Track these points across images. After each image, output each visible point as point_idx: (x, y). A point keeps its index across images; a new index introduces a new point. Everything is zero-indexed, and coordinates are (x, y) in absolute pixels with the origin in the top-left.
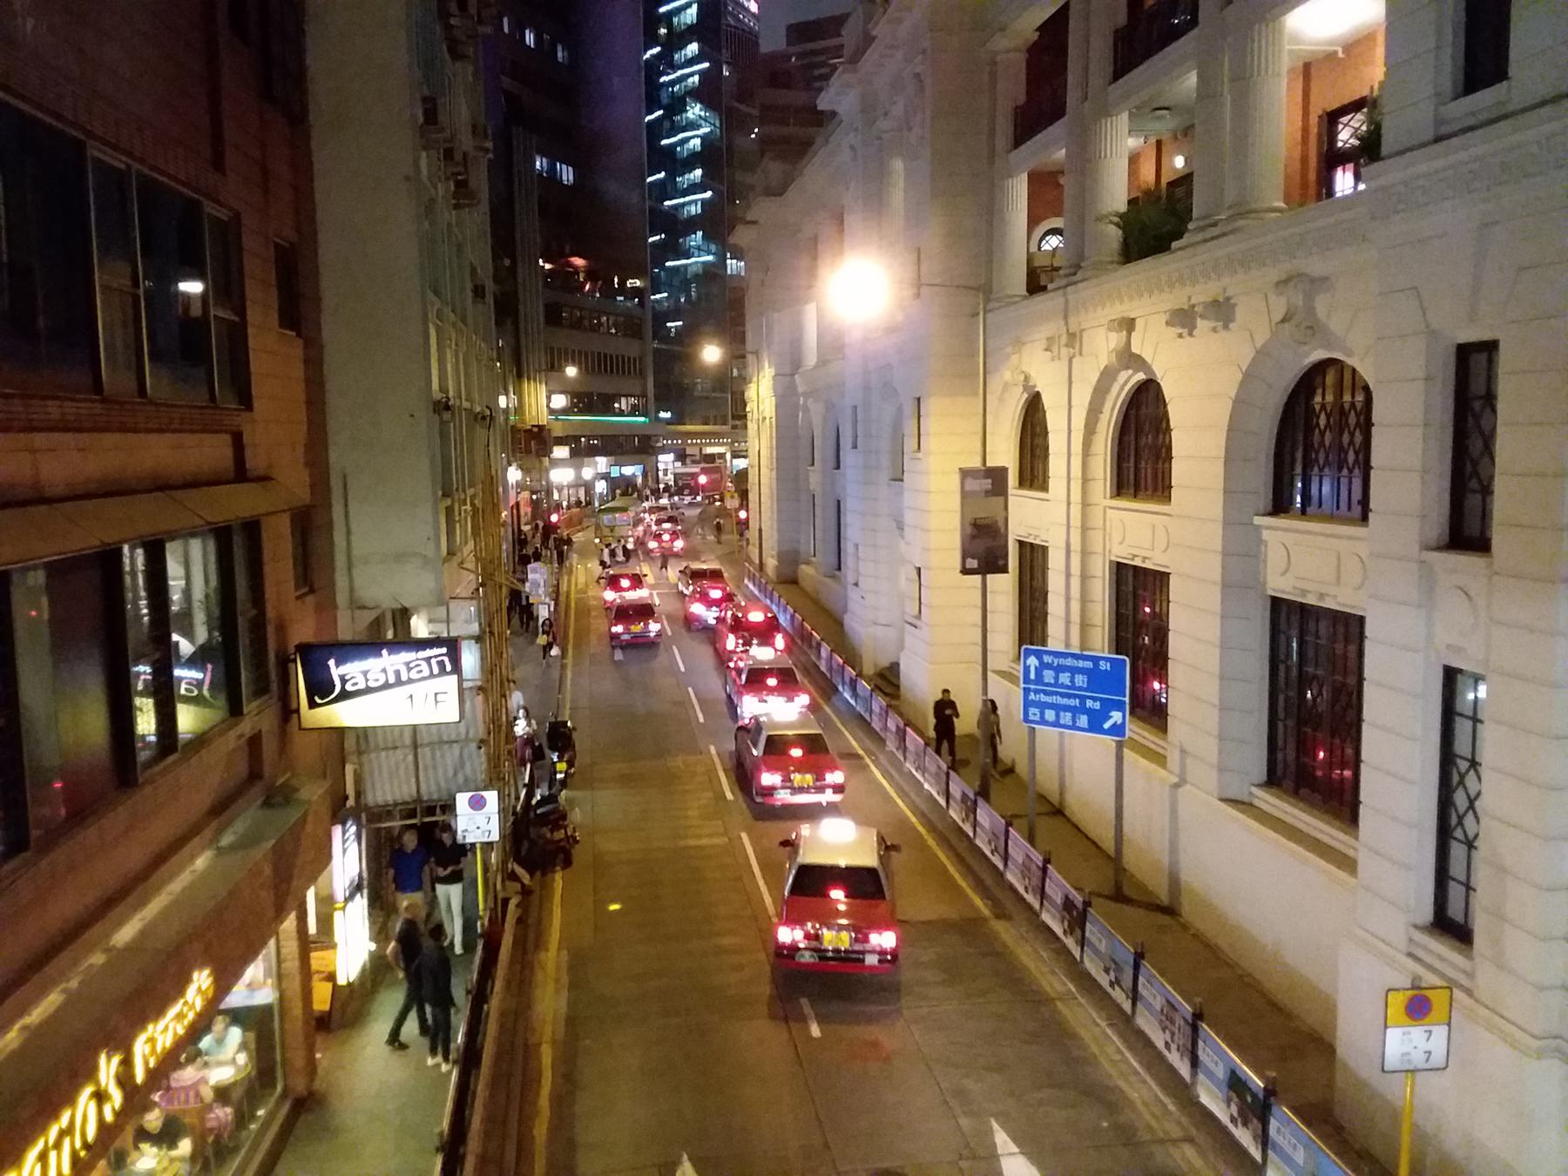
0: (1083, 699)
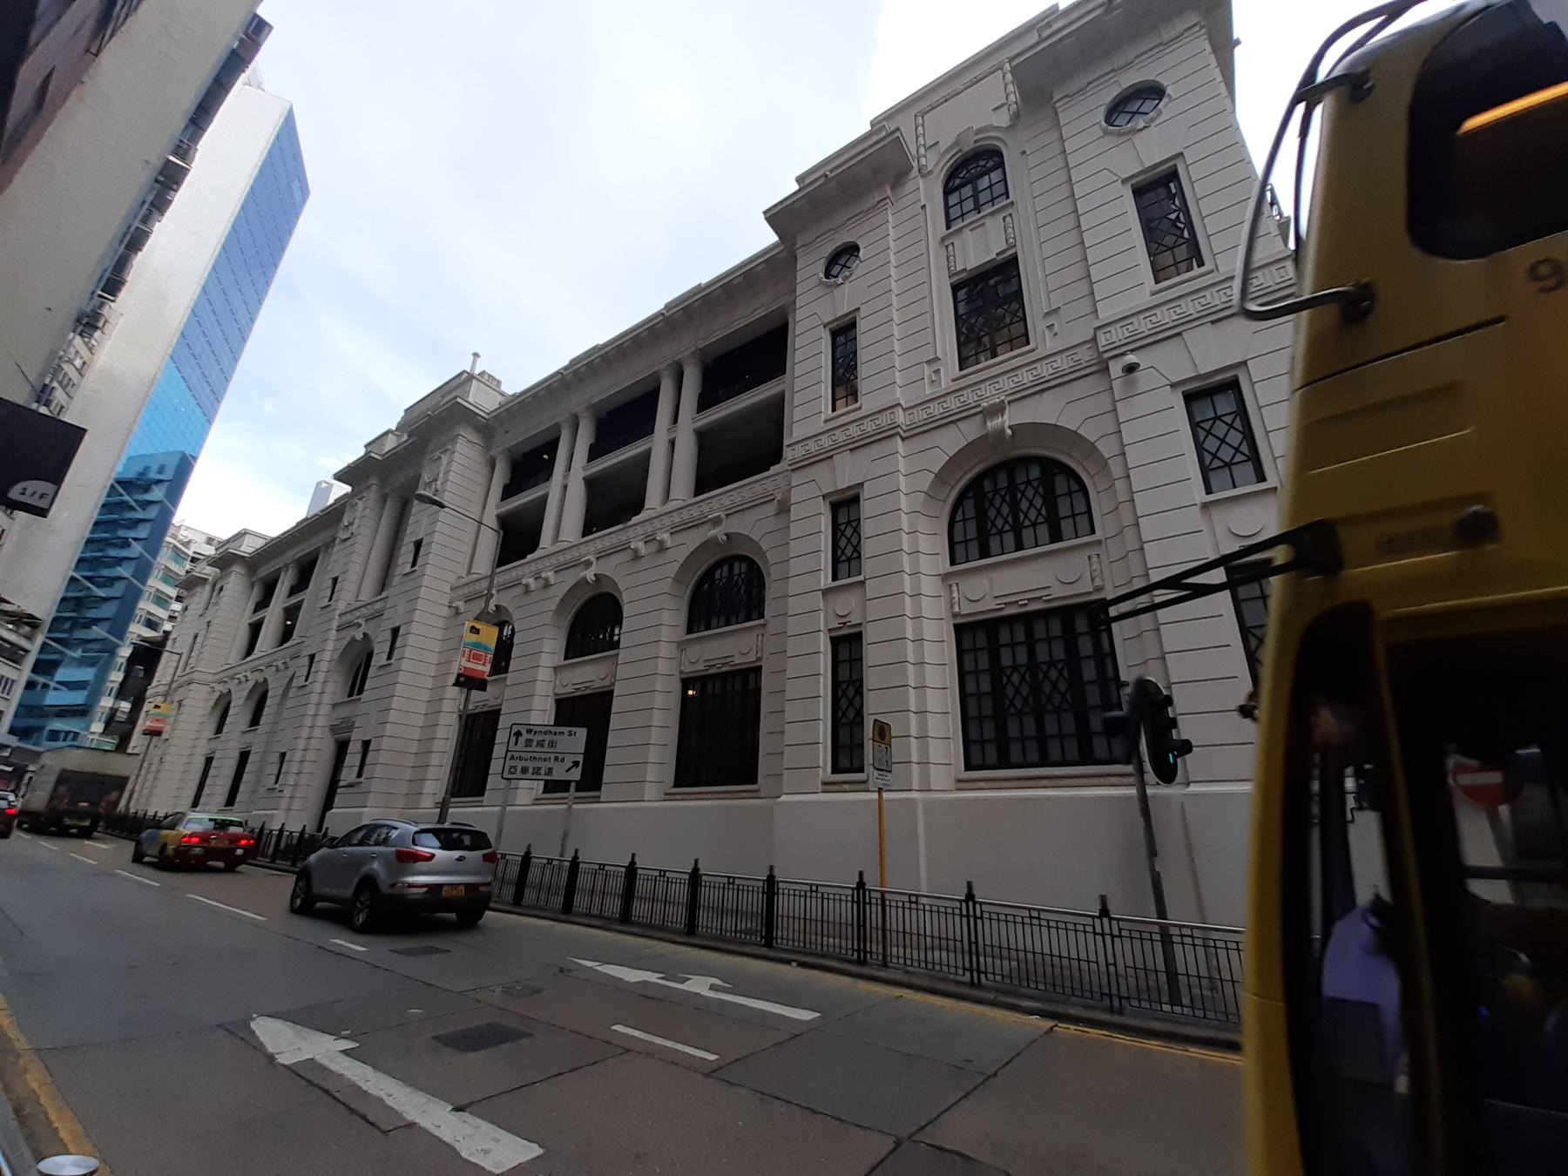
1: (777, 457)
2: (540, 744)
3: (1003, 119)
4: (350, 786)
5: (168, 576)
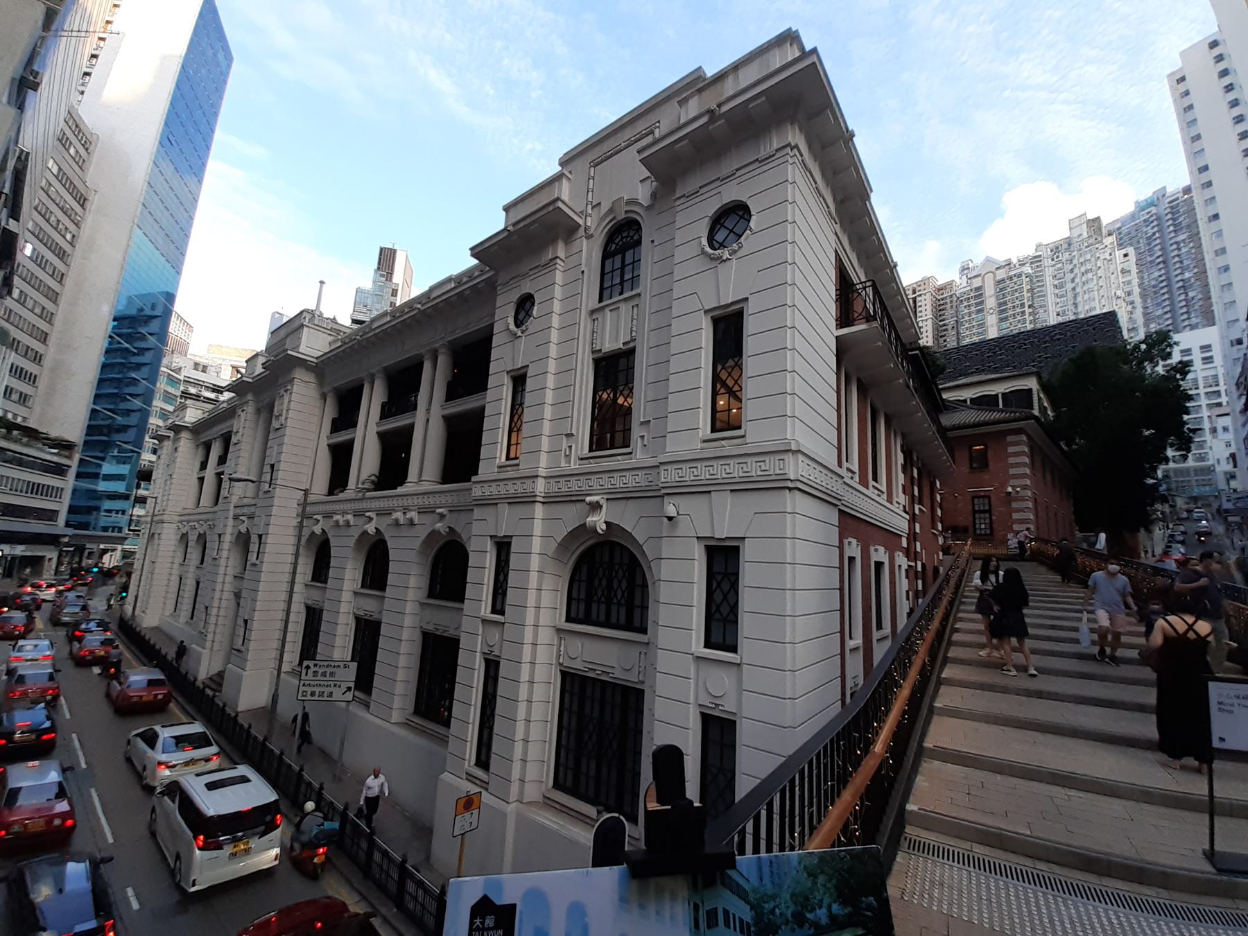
2: (324, 674)
3: (643, 193)
5: (168, 398)
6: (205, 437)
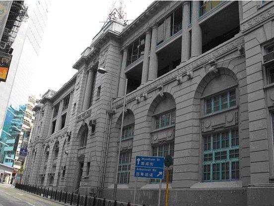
0: (152, 169)
1: (237, 30)
4: (85, 178)
6: (55, 103)
